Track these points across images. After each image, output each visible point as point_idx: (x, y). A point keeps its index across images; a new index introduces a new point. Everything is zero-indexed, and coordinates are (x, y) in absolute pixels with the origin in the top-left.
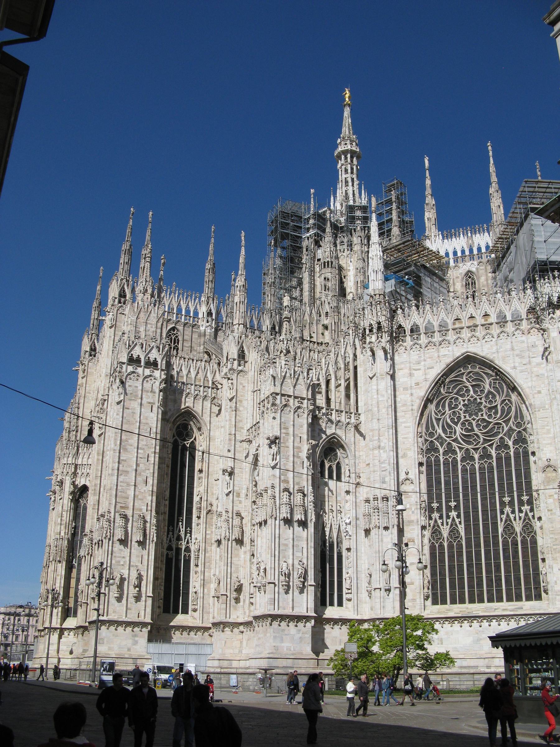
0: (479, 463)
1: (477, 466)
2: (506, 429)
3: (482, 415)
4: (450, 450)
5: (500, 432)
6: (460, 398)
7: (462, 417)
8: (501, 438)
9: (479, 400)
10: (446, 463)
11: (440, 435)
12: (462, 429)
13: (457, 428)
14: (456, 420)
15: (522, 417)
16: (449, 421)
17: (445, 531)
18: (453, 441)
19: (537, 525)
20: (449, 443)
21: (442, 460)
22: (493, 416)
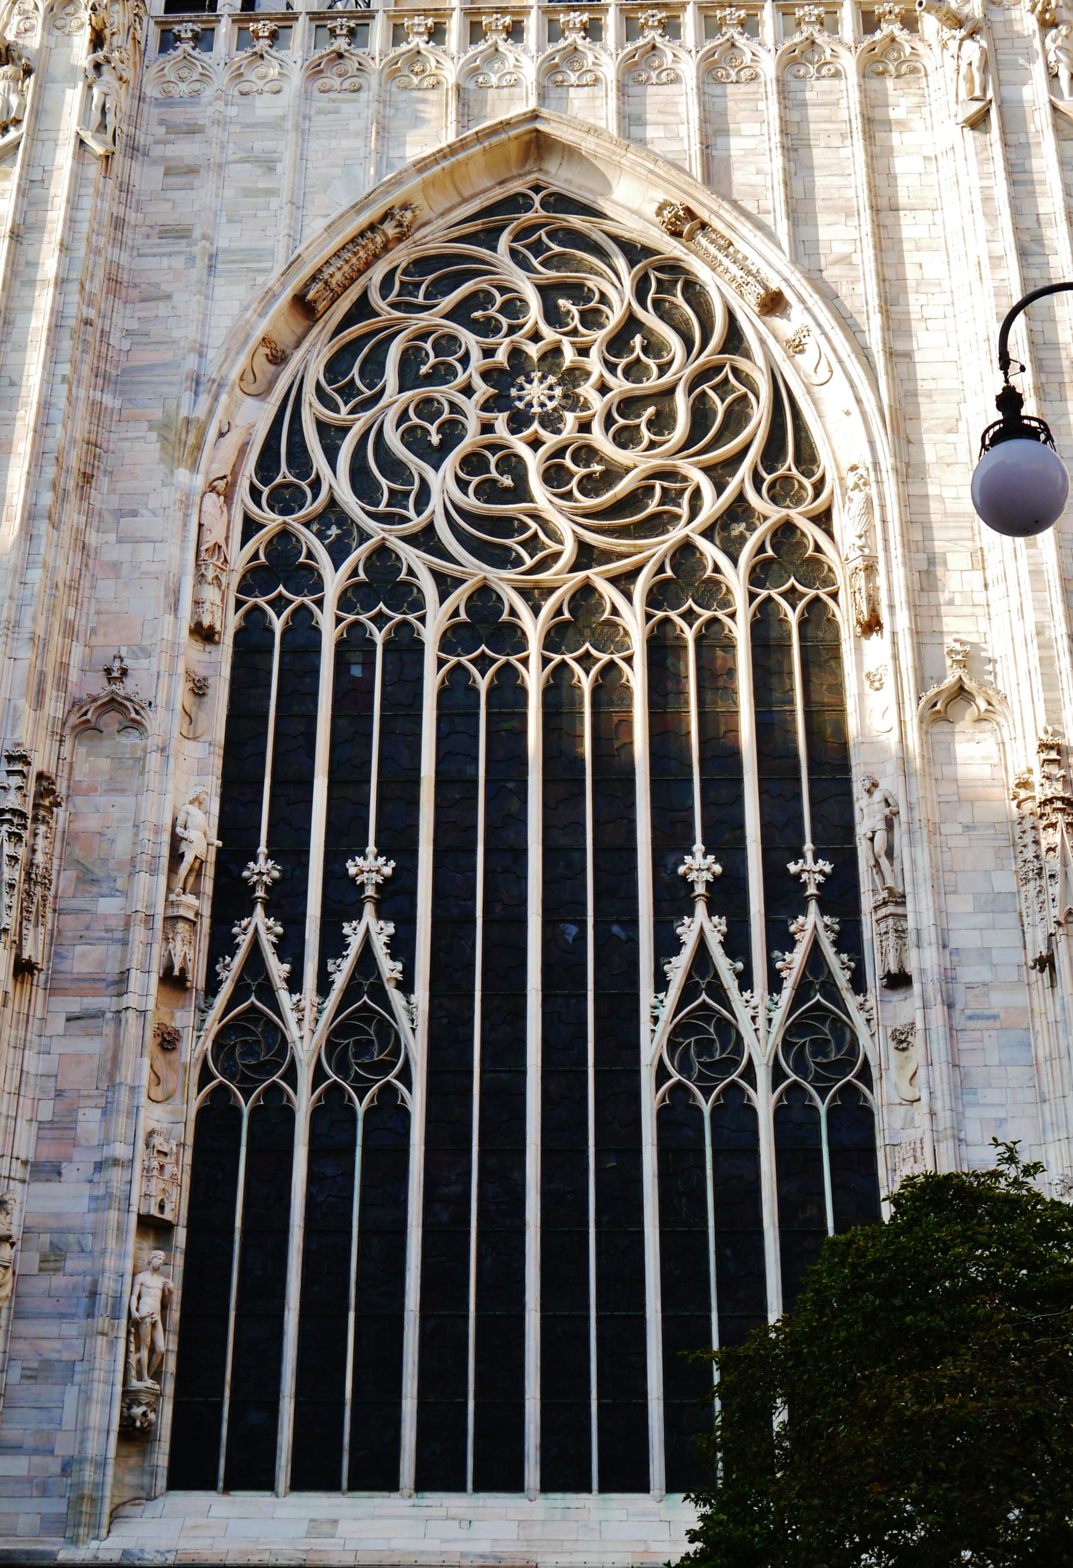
0: (546, 661)
1: (534, 680)
2: (712, 506)
3: (585, 427)
4: (383, 584)
5: (677, 517)
6: (469, 339)
7: (472, 425)
8: (687, 548)
9: (569, 356)
10: (353, 645)
11: (332, 502)
12: (463, 485)
13: (434, 479)
14: (435, 439)
15: (806, 458)
16: (393, 439)
17: (306, 1026)
18: (407, 539)
19: (871, 1018)
20: (382, 551)
21: (329, 636)
22: (646, 435)
